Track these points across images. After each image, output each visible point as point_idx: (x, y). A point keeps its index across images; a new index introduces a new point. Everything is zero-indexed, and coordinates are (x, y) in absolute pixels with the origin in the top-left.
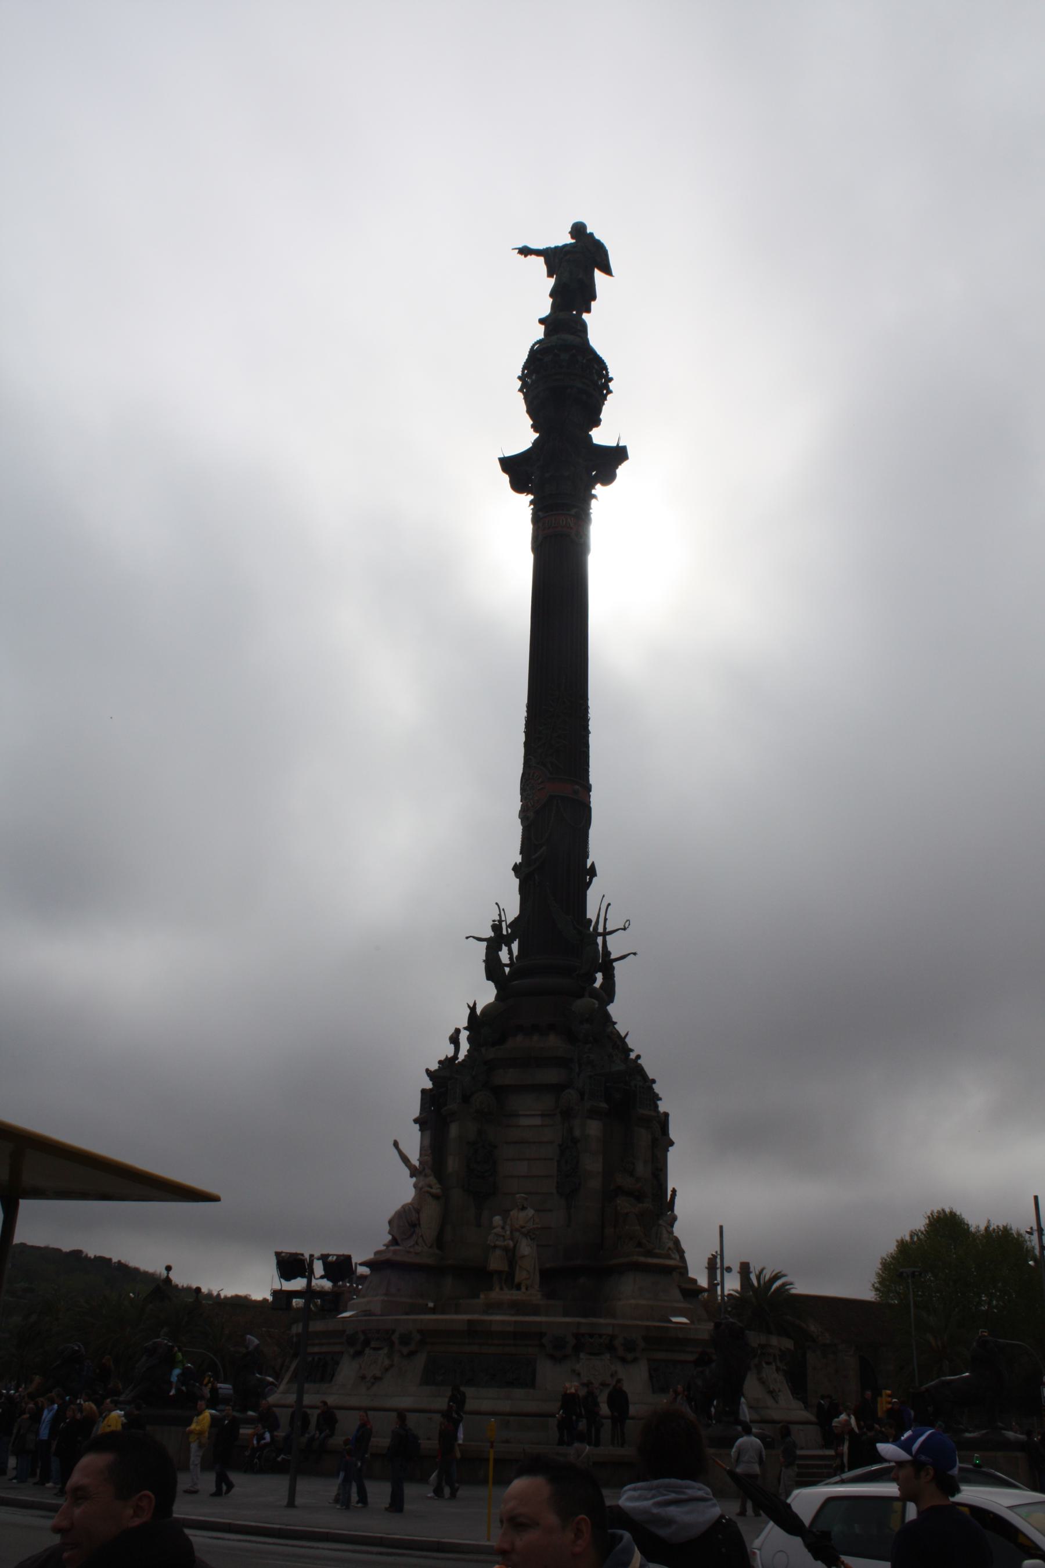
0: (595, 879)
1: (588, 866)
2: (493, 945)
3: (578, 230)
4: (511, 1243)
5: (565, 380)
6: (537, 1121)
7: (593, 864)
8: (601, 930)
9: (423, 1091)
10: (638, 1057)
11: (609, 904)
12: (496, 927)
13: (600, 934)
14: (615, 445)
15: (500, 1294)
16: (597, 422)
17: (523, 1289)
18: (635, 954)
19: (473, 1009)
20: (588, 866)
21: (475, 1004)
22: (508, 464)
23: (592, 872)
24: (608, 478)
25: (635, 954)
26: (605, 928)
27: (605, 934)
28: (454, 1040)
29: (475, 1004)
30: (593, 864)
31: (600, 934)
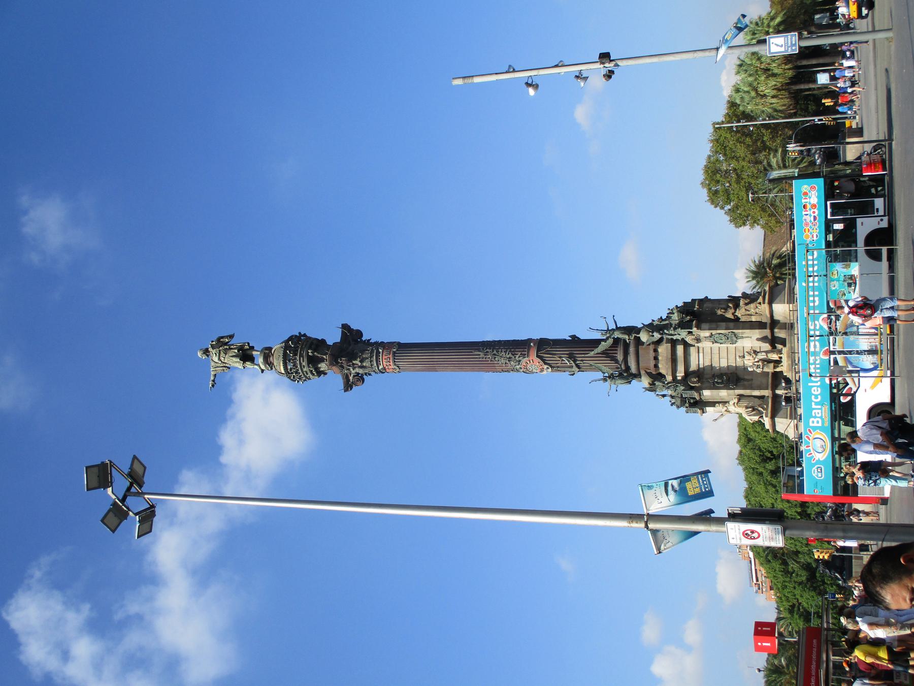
19: (647, 389)
22: (348, 386)
24: (359, 333)
28: (664, 396)
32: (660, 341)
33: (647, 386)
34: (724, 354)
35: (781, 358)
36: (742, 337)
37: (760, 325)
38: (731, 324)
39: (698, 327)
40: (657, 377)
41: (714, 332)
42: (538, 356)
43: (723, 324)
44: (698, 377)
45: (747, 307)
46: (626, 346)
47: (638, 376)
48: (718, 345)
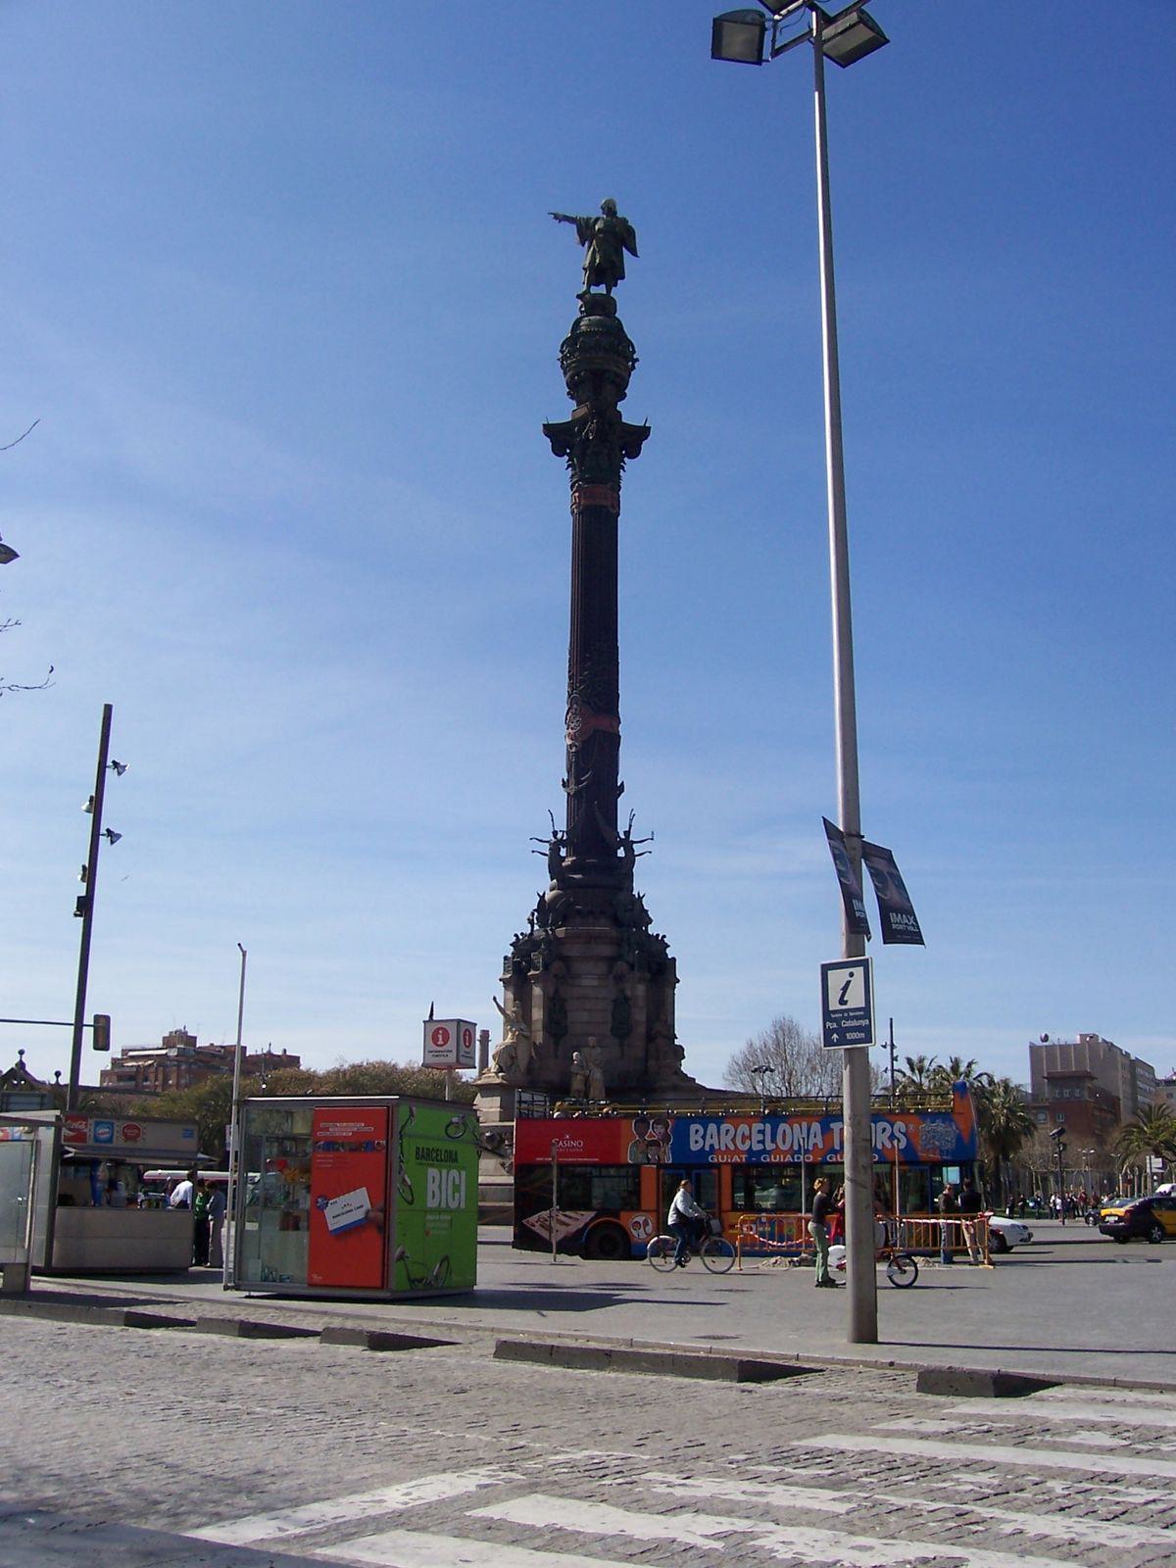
1: (619, 784)
2: (555, 847)
3: (610, 209)
5: (599, 359)
6: (596, 983)
7: (622, 783)
9: (506, 958)
10: (664, 936)
14: (642, 424)
16: (623, 396)
20: (619, 784)
21: (544, 894)
22: (550, 430)
23: (621, 788)
24: (634, 453)
28: (531, 922)
29: (544, 894)
30: (622, 783)
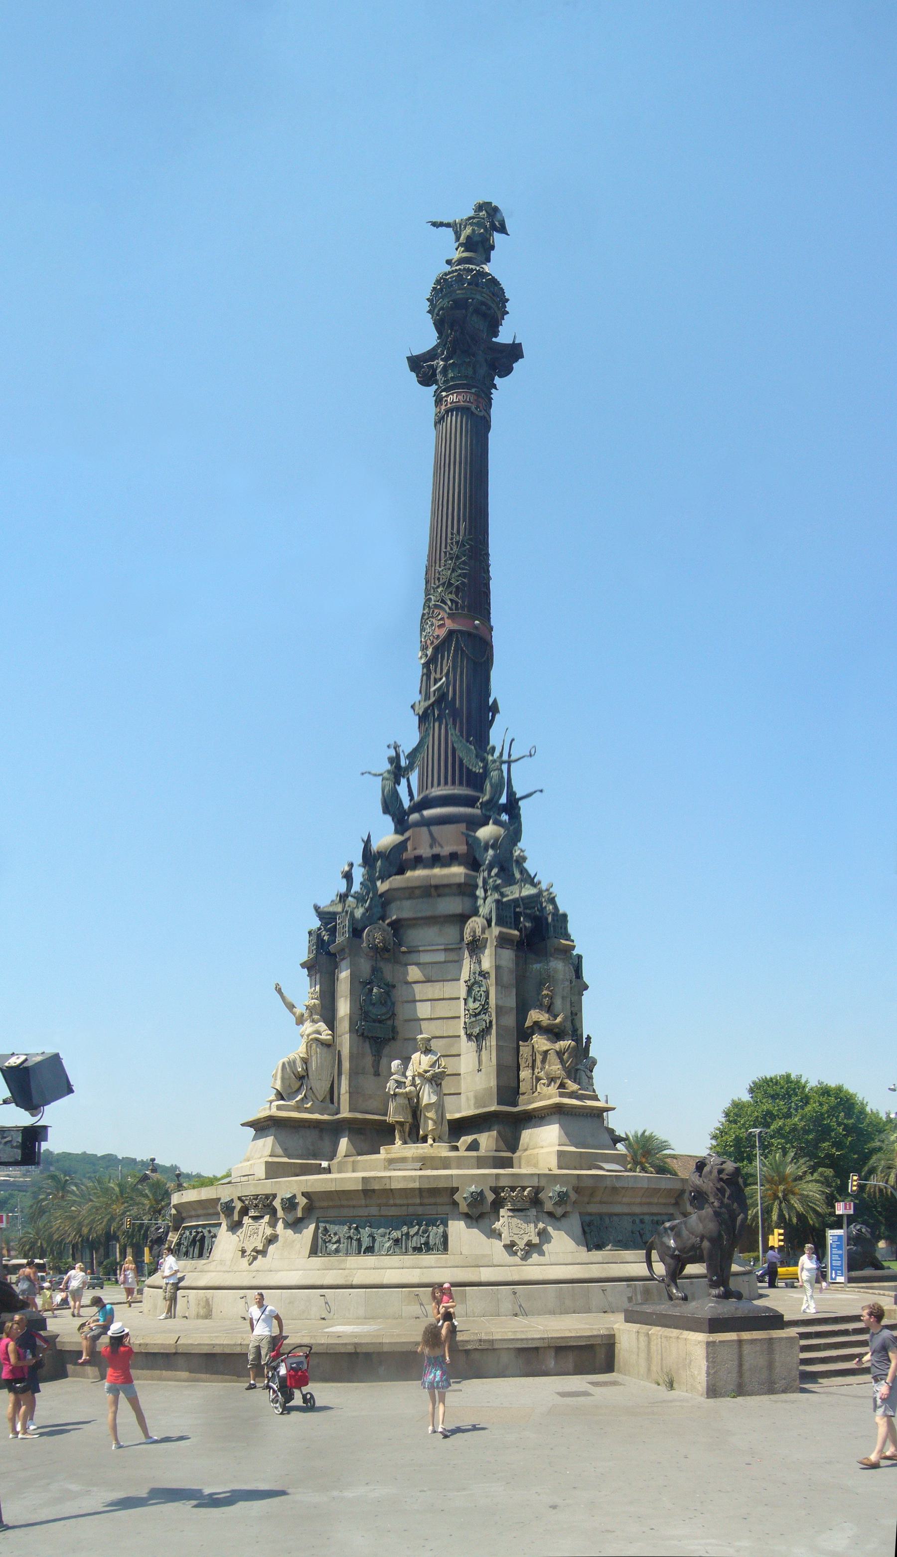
0: (497, 716)
4: (413, 1088)
6: (441, 957)
7: (495, 701)
8: (505, 757)
11: (513, 740)
12: (394, 761)
13: (504, 762)
15: (398, 1148)
17: (430, 1141)
18: (541, 791)
21: (369, 836)
23: (495, 709)
25: (541, 791)
26: (510, 756)
27: (509, 763)
28: (348, 876)
29: (369, 836)
30: (495, 701)
31: (504, 762)
32: (474, 865)
33: (375, 846)
34: (443, 1010)
35: (424, 1140)
36: (479, 1049)
37: (509, 1091)
38: (510, 1021)
39: (503, 941)
40: (393, 861)
41: (492, 981)
42: (451, 633)
43: (511, 1002)
44: (386, 949)
45: (552, 1057)
46: (470, 802)
47: (401, 825)
48: (463, 994)
